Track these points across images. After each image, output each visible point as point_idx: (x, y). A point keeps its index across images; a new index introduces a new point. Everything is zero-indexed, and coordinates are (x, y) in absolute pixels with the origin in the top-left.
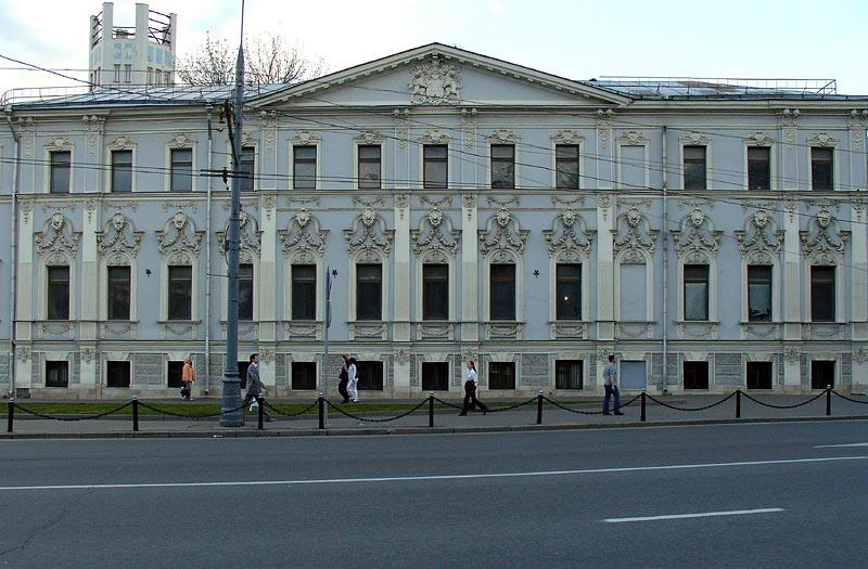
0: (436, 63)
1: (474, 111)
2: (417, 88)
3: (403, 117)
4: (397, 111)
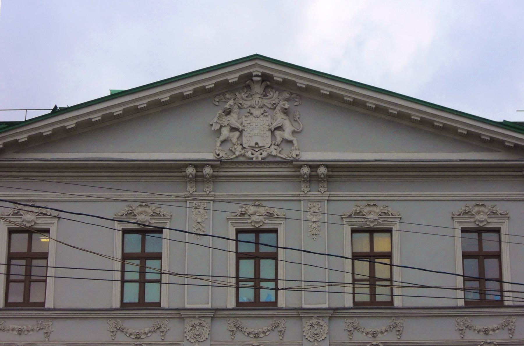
0: (258, 89)
1: (322, 170)
2: (225, 132)
3: (198, 179)
4: (191, 170)
